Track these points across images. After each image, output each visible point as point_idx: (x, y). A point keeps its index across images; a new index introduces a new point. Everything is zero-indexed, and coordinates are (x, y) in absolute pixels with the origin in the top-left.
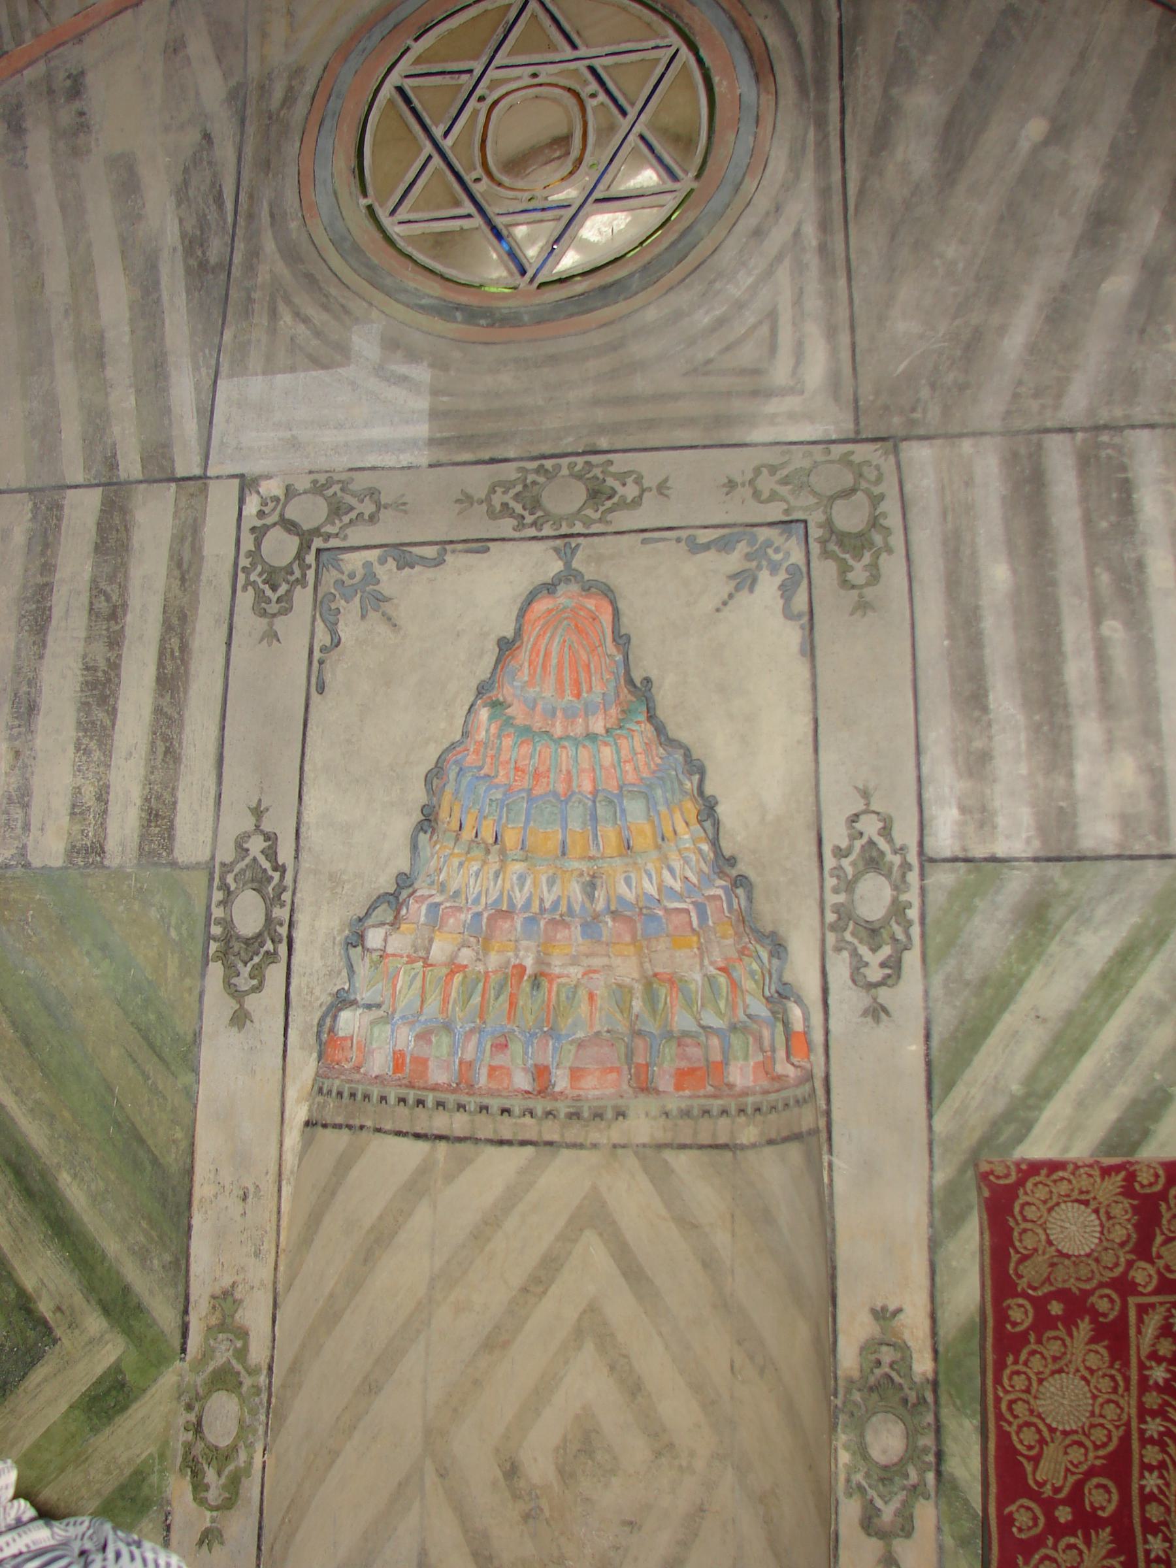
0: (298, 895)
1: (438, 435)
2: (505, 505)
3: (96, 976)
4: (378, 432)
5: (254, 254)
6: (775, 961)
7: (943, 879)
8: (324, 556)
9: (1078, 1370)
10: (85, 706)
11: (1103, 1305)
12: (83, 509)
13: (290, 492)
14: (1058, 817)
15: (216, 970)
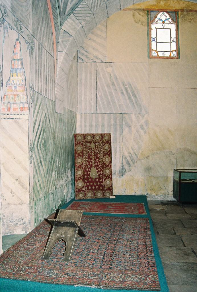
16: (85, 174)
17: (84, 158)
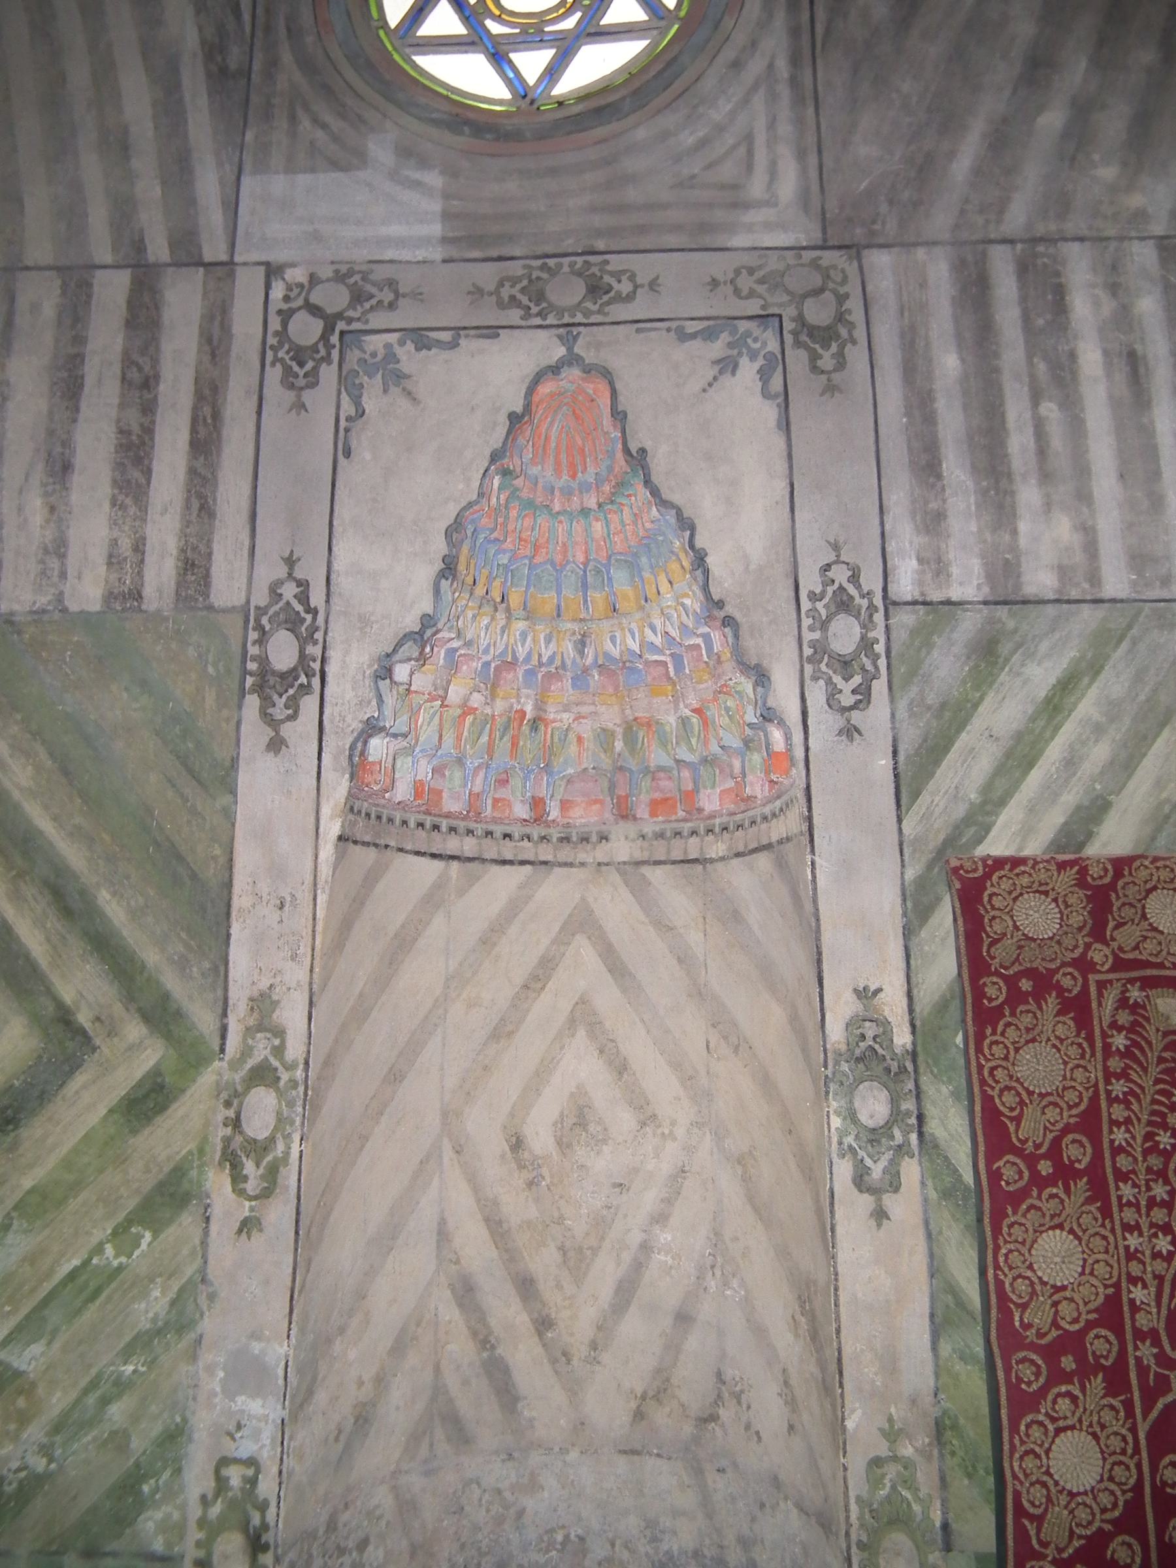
0: (330, 634)
1: (451, 235)
2: (513, 298)
3: (135, 710)
4: (396, 230)
5: (273, 64)
6: (759, 689)
7: (905, 619)
8: (347, 338)
9: (1049, 1040)
10: (119, 466)
11: (1067, 982)
12: (112, 289)
13: (314, 280)
14: (1004, 570)
15: (253, 701)
16: (1159, 1491)
17: (1129, 1215)
